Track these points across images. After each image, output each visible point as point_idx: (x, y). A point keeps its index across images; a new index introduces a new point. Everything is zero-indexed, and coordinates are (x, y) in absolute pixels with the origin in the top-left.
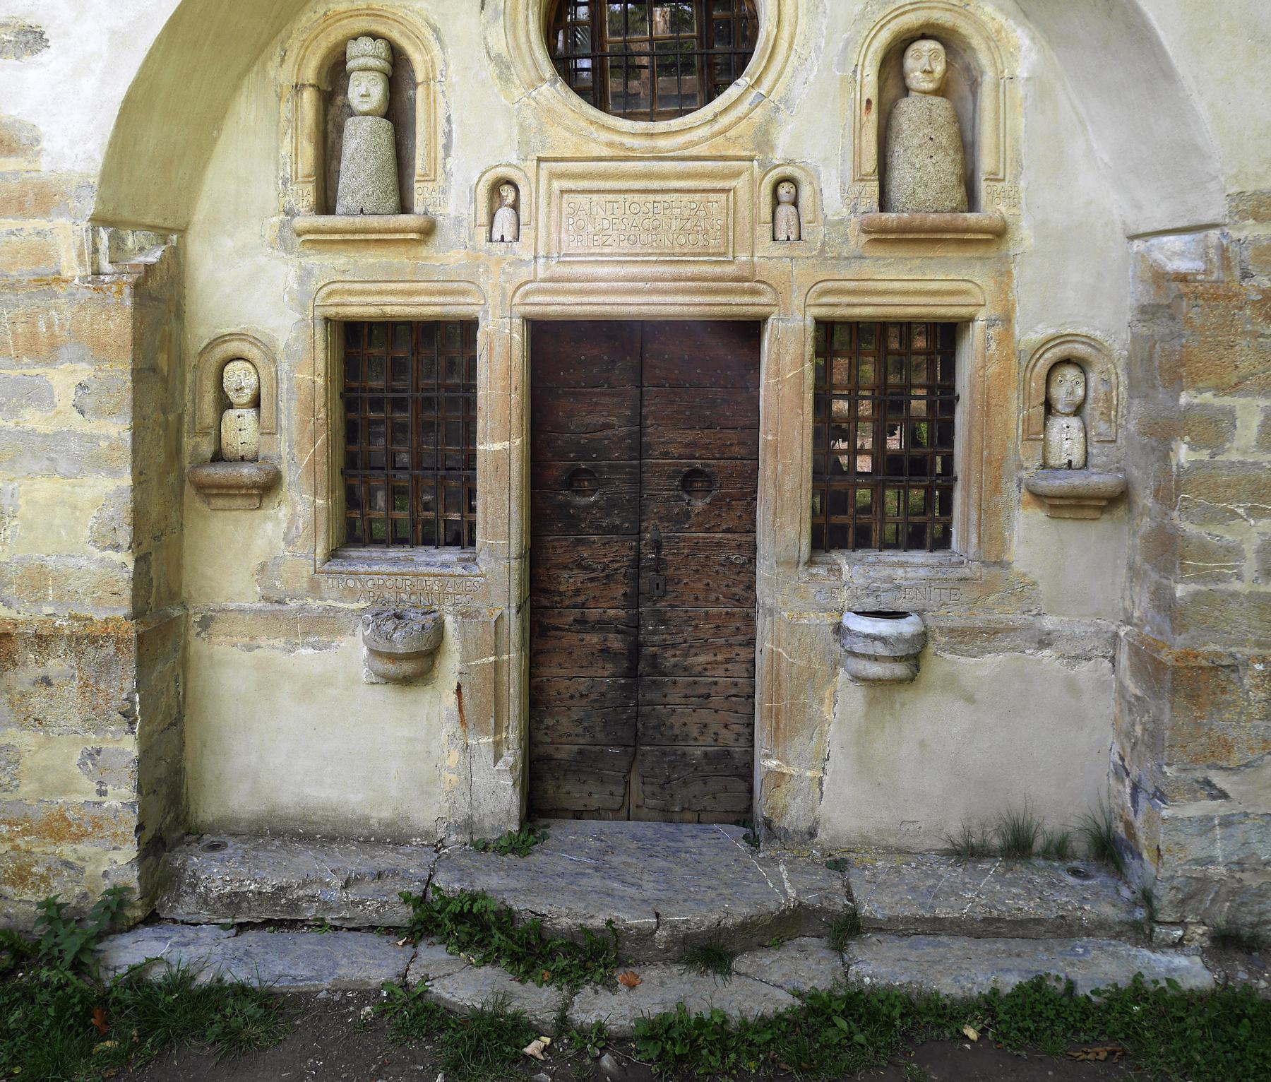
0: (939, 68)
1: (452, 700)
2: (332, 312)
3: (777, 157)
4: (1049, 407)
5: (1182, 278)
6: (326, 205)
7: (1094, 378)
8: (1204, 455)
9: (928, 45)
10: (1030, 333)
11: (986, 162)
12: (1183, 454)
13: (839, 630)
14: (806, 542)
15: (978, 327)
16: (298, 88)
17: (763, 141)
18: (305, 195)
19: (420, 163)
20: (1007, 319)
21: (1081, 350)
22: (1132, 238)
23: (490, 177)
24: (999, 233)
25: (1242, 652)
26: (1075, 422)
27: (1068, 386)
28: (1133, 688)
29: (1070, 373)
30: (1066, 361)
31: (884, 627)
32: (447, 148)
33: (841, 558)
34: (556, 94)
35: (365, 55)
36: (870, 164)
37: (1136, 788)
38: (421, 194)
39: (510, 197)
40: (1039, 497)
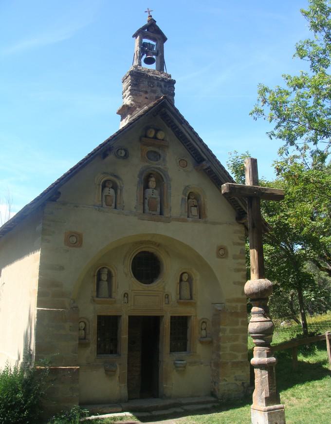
0: (187, 278)
1: (118, 378)
2: (99, 314)
3: (166, 291)
4: (202, 329)
5: (220, 310)
6: (97, 296)
7: (207, 324)
8: (223, 334)
9: (185, 274)
10: (199, 317)
11: (194, 292)
12: (221, 335)
13: (175, 364)
14: (169, 351)
15: (192, 317)
16: (94, 276)
17: (164, 289)
18: (95, 294)
19: (113, 289)
20: (196, 316)
21: (204, 320)
22: (213, 304)
23: (124, 293)
24: (195, 303)
25: (228, 361)
26: (205, 331)
27: (204, 326)
28: (214, 368)
29: (204, 324)
30: (204, 322)
31: (182, 362)
32: (118, 287)
33: (173, 353)
34: (134, 279)
35: (106, 271)
36: (178, 293)
37: (215, 383)
38: (114, 295)
39: (126, 295)
40: (201, 342)
